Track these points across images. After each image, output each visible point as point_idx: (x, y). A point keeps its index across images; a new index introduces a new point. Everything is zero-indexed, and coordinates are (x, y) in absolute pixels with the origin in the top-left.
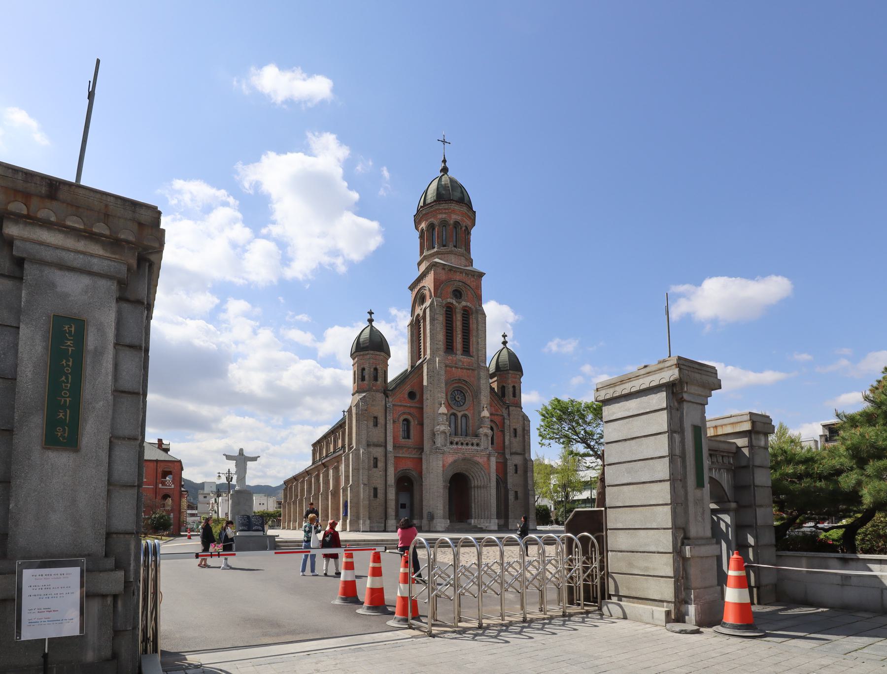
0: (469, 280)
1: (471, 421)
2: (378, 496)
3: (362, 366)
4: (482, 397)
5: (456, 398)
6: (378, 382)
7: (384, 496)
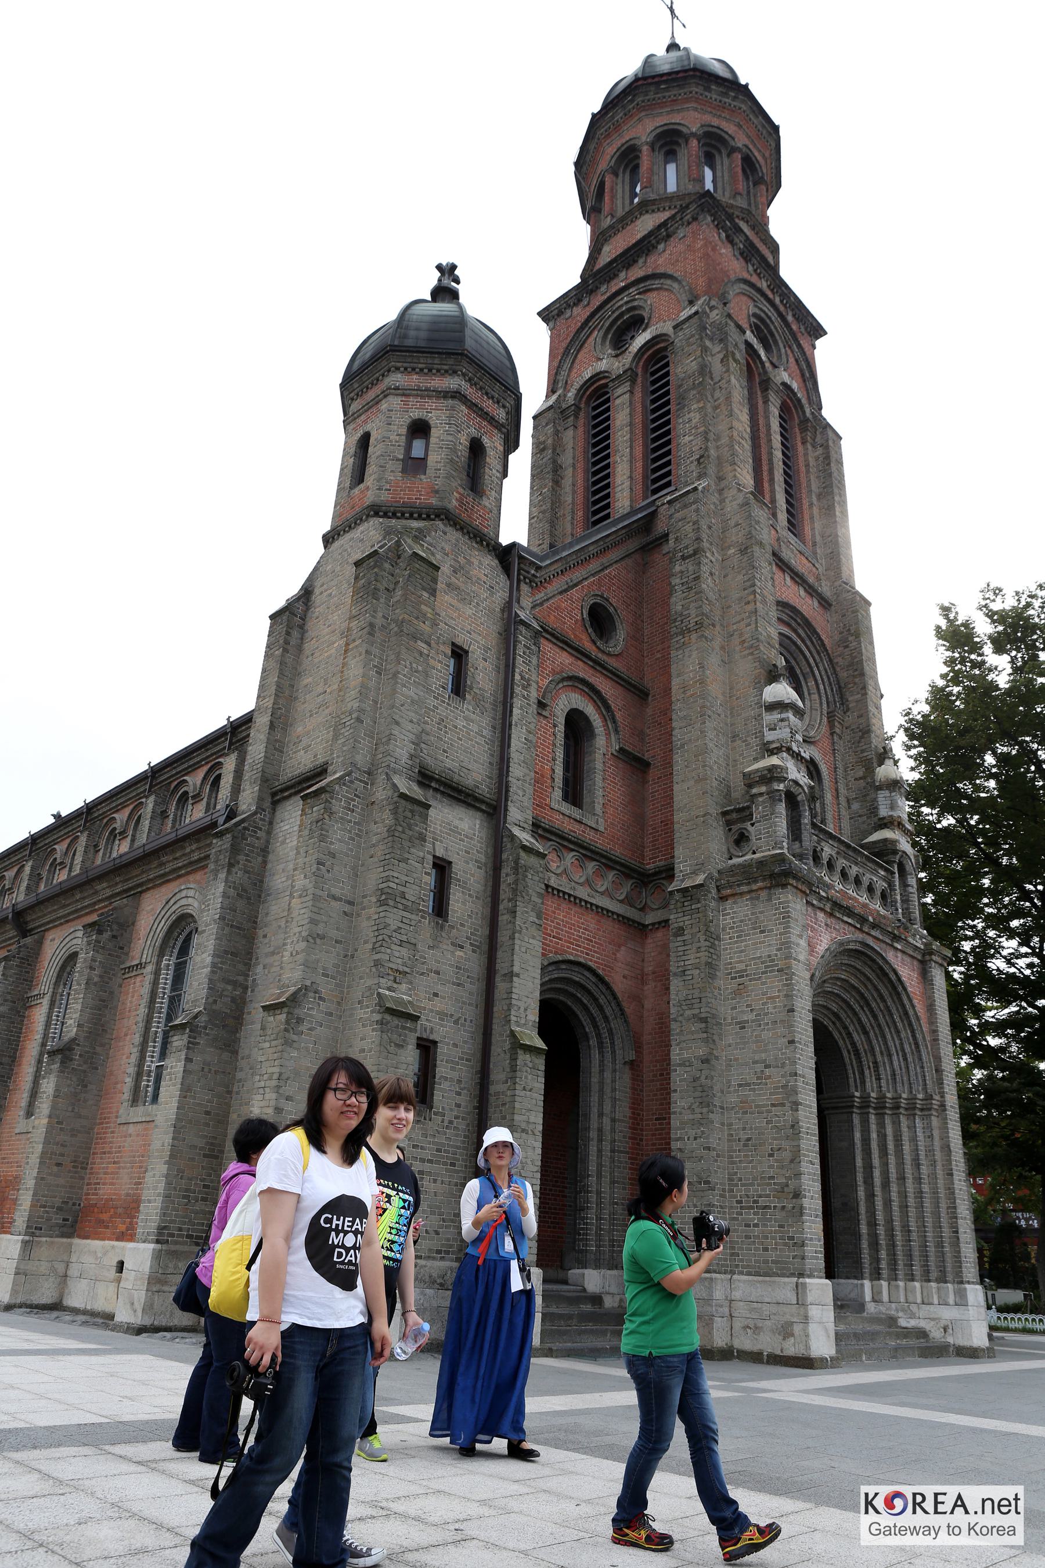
2: (438, 1096)
3: (416, 414)
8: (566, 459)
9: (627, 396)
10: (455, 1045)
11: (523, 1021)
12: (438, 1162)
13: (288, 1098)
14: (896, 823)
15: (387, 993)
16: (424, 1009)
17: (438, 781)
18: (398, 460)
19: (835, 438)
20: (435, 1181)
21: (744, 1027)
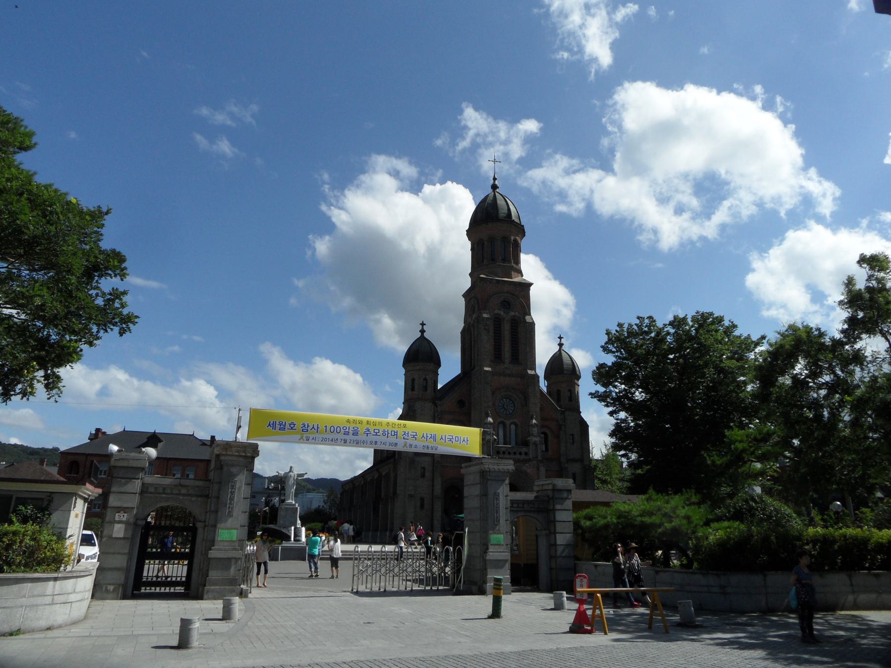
5: (505, 406)
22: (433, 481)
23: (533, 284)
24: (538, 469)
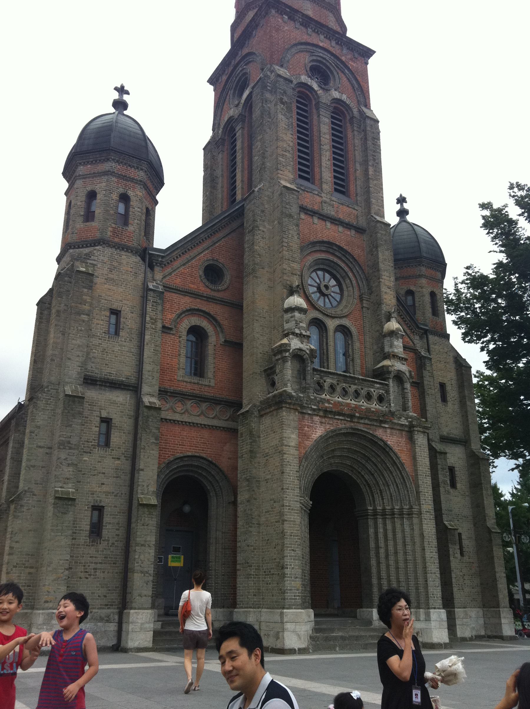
0: (345, 56)
1: (357, 345)
3: (89, 188)
4: (384, 289)
5: (323, 289)
6: (131, 228)
7: (122, 532)
8: (218, 172)
9: (240, 131)
10: (115, 507)
11: (146, 492)
12: (105, 563)
13: (17, 542)
14: (391, 356)
15: (60, 489)
16: (96, 492)
17: (100, 381)
18: (81, 216)
19: (372, 123)
20: (104, 572)
21: (267, 482)
22: (134, 458)
23: (374, 52)
24: (411, 440)
